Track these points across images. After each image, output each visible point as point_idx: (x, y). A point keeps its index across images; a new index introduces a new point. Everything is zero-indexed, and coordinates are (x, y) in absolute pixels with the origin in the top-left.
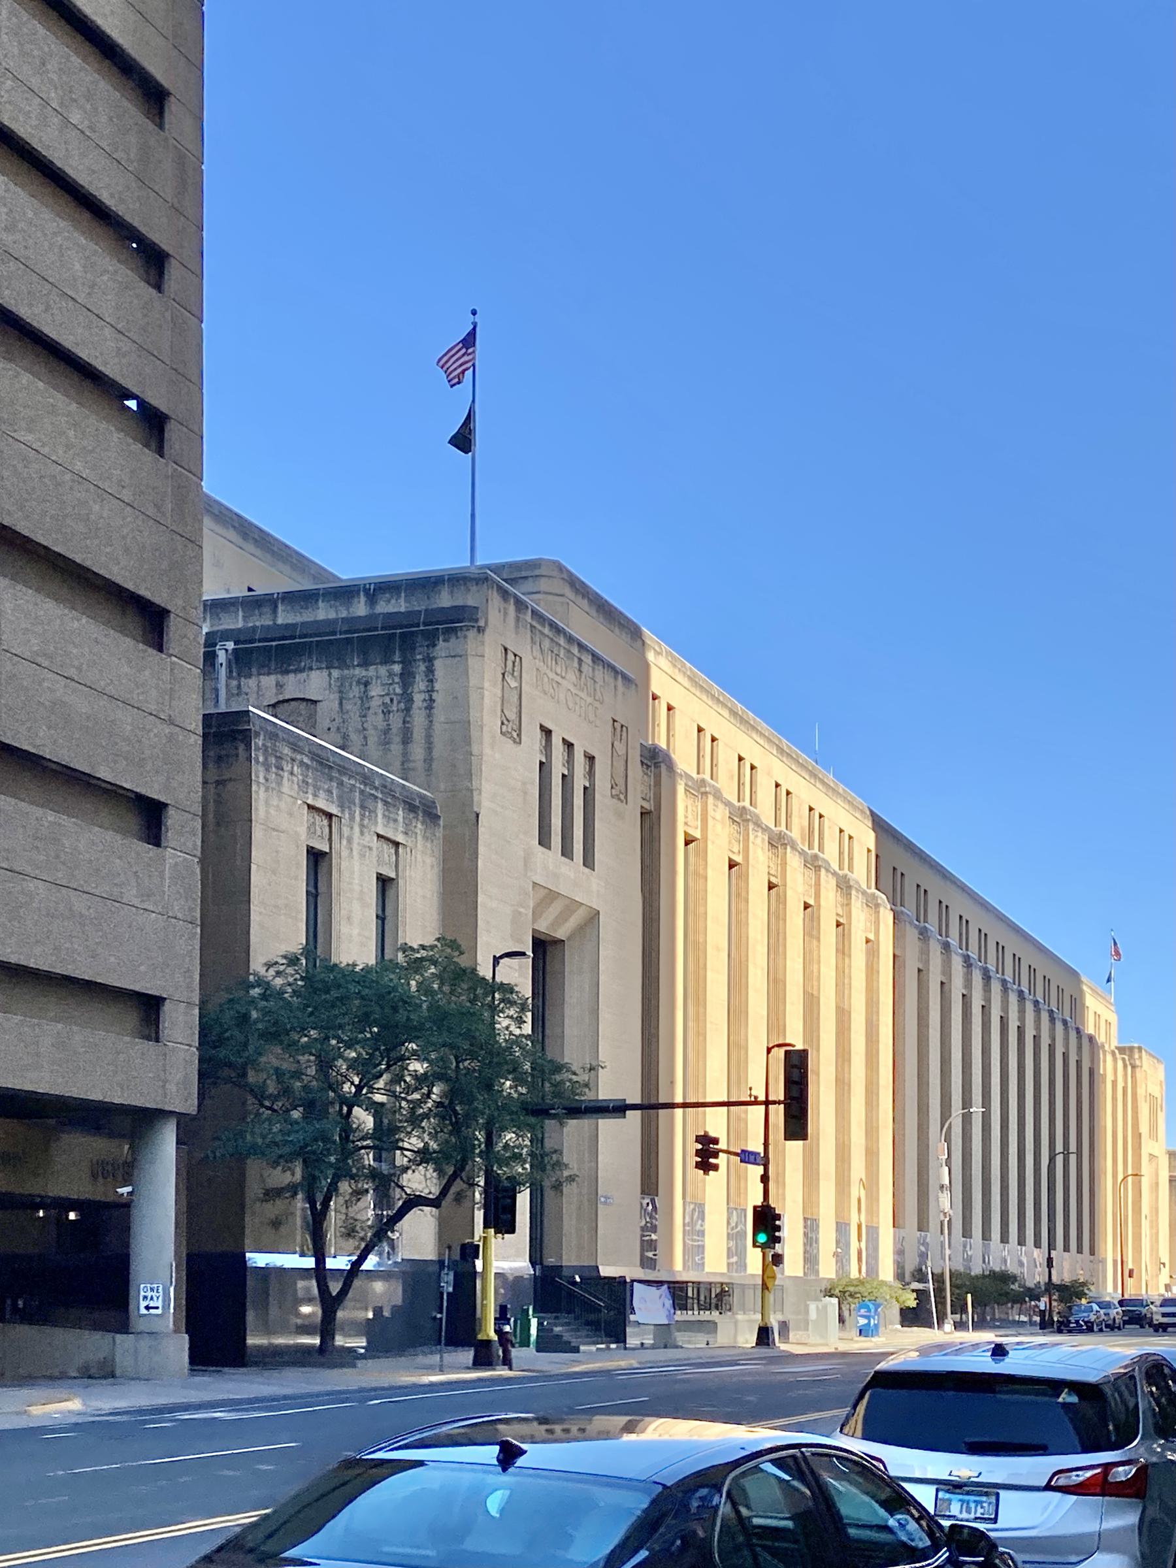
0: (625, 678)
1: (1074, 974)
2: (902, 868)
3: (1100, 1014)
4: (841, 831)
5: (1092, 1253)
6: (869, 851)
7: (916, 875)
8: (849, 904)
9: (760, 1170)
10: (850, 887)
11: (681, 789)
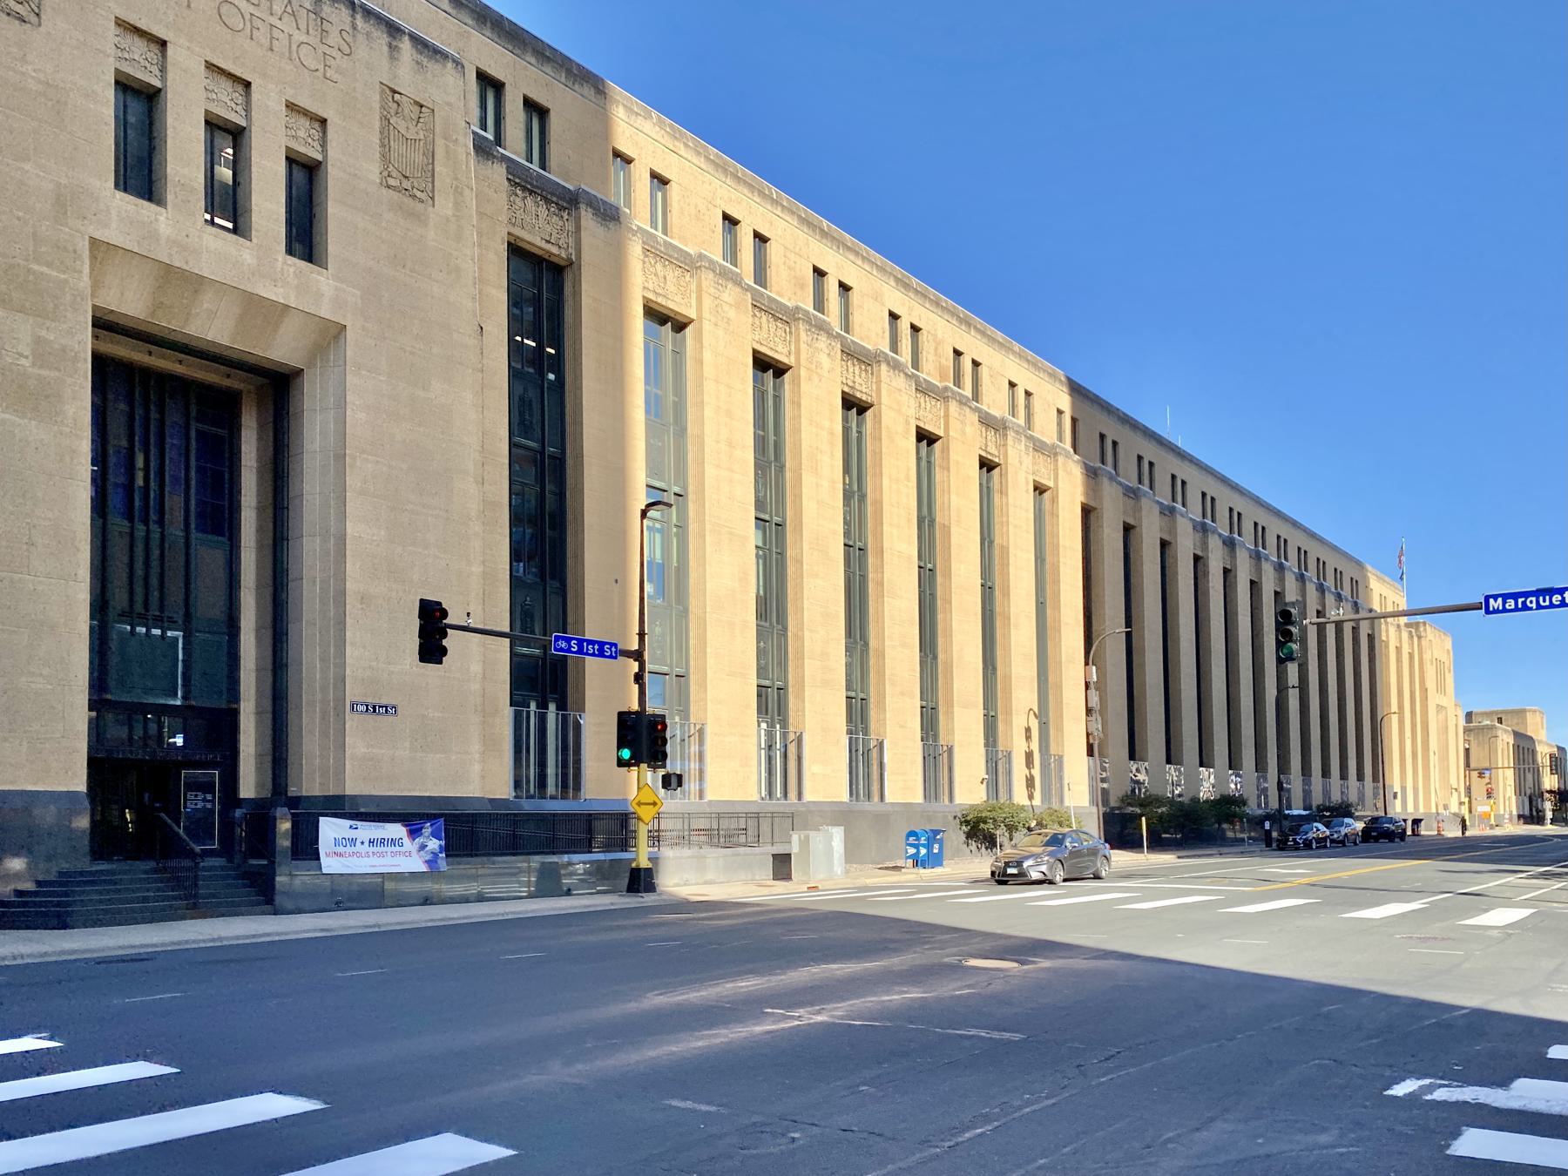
0: (417, 41)
1: (1359, 564)
2: (1102, 433)
3: (1383, 593)
4: (1012, 385)
5: (1375, 779)
6: (1060, 412)
7: (1132, 445)
8: (1005, 445)
9: (635, 666)
10: (1005, 428)
11: (635, 249)
